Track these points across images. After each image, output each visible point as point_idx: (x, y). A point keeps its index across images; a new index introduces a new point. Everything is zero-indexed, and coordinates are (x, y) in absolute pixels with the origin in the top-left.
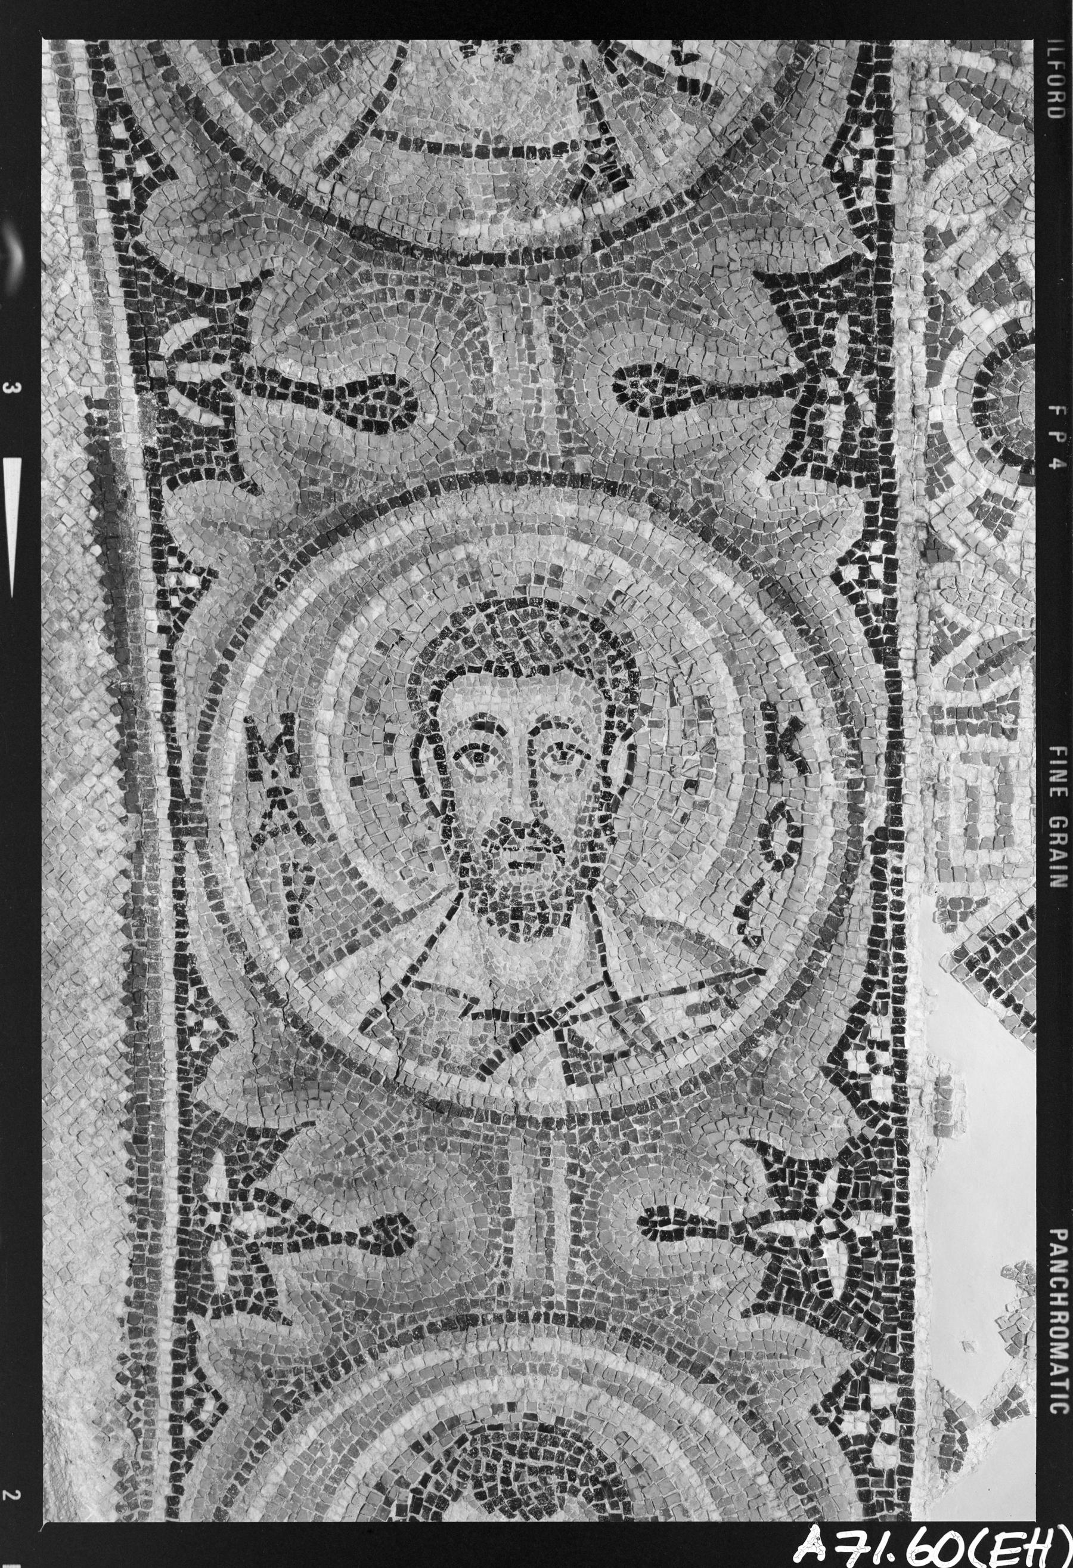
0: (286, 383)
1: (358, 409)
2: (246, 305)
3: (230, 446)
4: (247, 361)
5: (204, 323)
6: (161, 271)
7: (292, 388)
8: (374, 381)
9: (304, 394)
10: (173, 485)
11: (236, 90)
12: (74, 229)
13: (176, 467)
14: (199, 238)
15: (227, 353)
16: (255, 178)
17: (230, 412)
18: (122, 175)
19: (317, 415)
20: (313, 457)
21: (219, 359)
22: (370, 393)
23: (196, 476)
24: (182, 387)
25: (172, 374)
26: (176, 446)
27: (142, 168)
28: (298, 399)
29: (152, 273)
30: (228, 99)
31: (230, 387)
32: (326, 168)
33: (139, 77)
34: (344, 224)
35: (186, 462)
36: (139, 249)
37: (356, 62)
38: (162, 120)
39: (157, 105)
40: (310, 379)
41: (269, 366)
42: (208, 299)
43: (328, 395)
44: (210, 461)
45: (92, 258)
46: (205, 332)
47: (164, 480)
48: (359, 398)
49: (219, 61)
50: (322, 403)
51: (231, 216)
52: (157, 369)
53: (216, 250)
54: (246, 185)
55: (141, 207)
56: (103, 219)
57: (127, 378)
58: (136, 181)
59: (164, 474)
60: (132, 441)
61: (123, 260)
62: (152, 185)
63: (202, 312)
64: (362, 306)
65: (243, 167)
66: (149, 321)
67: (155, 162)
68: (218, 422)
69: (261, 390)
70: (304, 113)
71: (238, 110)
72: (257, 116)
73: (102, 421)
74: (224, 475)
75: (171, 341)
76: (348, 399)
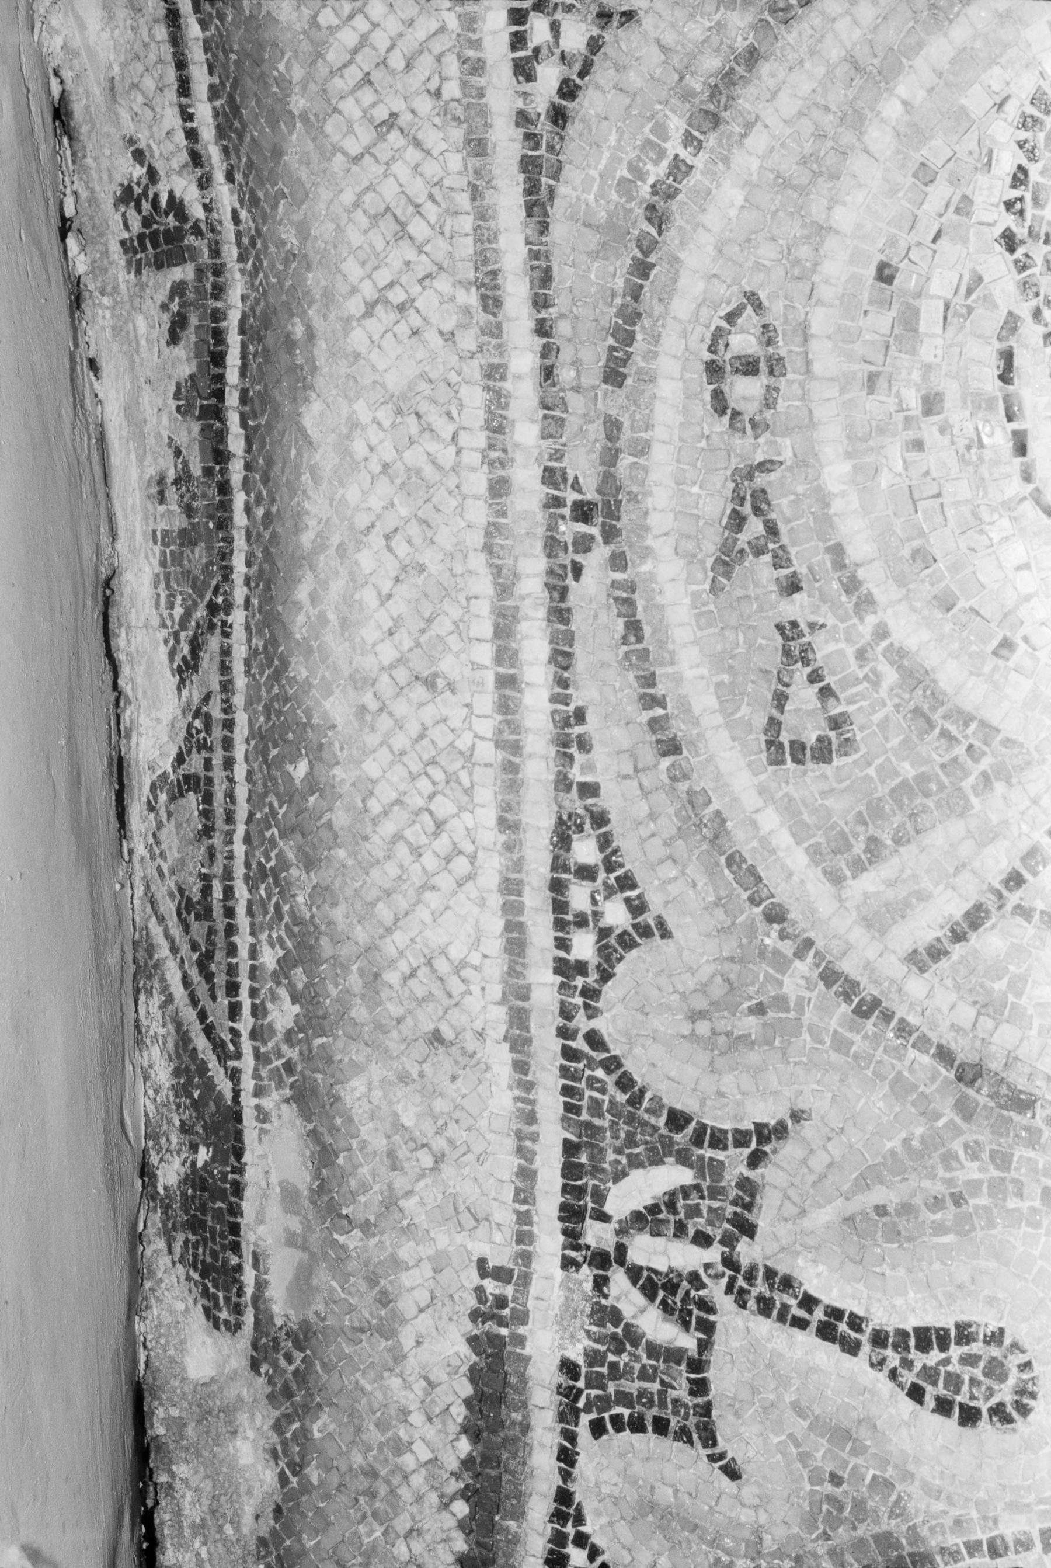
0: (809, 1302)
1: (930, 1374)
2: (755, 1160)
3: (700, 1387)
4: (746, 1251)
5: (685, 1176)
6: (625, 1083)
7: (819, 1314)
8: (964, 1334)
9: (836, 1328)
10: (598, 1429)
11: (789, 809)
12: (496, 991)
13: (604, 1403)
14: (693, 1037)
15: (718, 1234)
16: (799, 954)
17: (707, 1328)
18: (581, 921)
19: (859, 1365)
20: (841, 1436)
21: (703, 1240)
22: (956, 1351)
23: (637, 1426)
24: (634, 1273)
25: (621, 1250)
26: (613, 1366)
27: (616, 915)
28: (826, 1332)
29: (610, 1080)
30: (770, 820)
31: (716, 1291)
32: (927, 957)
33: (628, 768)
34: (944, 1055)
35: (624, 1398)
36: (594, 1040)
37: (999, 787)
38: (657, 841)
39: (652, 816)
40: (849, 1305)
41: (782, 1269)
42: (698, 1140)
43: (879, 1339)
44: (663, 1404)
45: (519, 1043)
46: (685, 1191)
47: (585, 1419)
48: (935, 1356)
49: (764, 756)
50: (866, 1348)
51: (751, 1011)
52: (597, 1235)
53: (720, 1062)
54: (781, 963)
55: (606, 976)
56: (543, 981)
57: (549, 1241)
58: (604, 933)
59: (587, 1409)
60: (550, 1339)
61: (569, 1054)
62: (627, 942)
63: (683, 1159)
64: (958, 1200)
65: (783, 936)
66: (596, 1153)
67: (637, 908)
68: (688, 1342)
69: (765, 1307)
70: (895, 861)
71: (783, 839)
72: (815, 854)
73: (501, 1302)
74: (684, 1435)
75: (630, 1194)
76: (914, 1354)
